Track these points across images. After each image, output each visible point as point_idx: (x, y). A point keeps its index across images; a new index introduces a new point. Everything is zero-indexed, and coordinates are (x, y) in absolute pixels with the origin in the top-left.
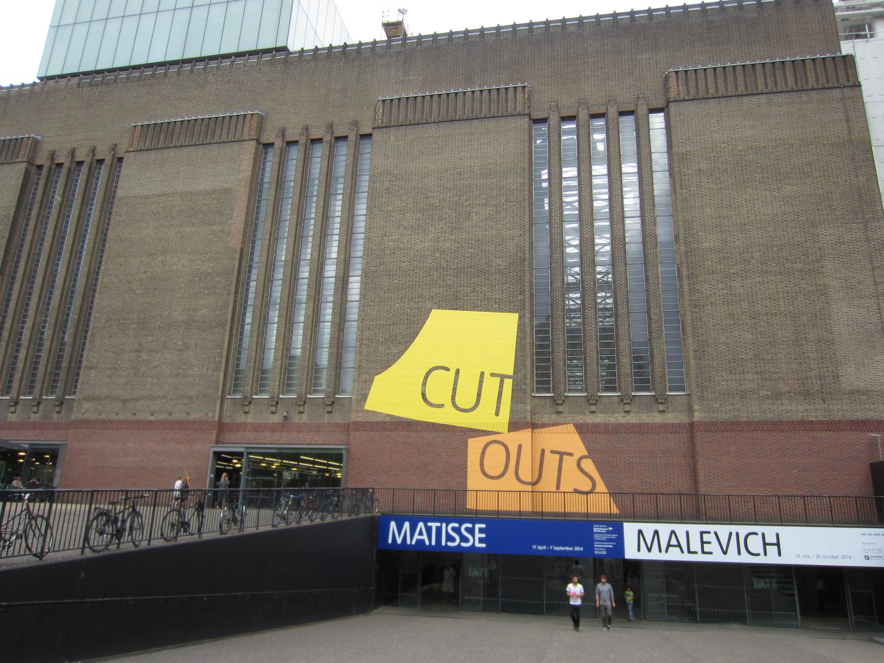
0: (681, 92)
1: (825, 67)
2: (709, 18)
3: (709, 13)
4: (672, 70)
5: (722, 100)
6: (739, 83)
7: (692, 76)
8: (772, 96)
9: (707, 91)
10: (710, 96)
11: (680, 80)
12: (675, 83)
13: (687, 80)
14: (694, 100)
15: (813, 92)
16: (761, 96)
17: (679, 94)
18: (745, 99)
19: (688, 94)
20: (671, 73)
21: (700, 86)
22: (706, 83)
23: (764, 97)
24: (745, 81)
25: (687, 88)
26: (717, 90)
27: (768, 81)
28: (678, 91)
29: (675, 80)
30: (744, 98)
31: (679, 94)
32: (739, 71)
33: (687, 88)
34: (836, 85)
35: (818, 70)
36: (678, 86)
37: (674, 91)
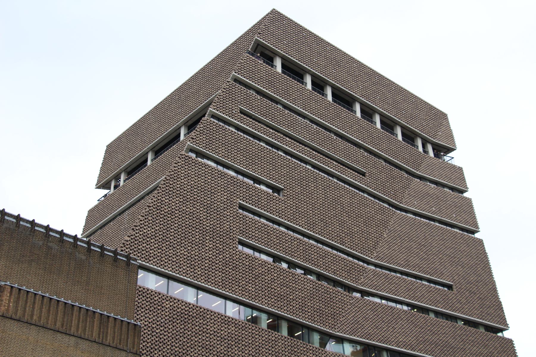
0: (11, 308)
1: (121, 329)
2: (49, 244)
3: (50, 239)
4: (8, 283)
5: (42, 330)
6: (58, 318)
7: (23, 296)
8: (80, 341)
9: (32, 315)
10: (33, 322)
11: (13, 297)
12: (8, 298)
13: (18, 298)
14: (19, 320)
15: (109, 348)
16: (71, 338)
17: (8, 310)
18: (59, 336)
19: (16, 314)
20: (7, 287)
21: (27, 309)
22: (33, 308)
23: (73, 339)
24: (63, 318)
25: (17, 307)
26: (40, 318)
27: (80, 326)
28: (9, 306)
29: (8, 295)
30: (59, 335)
31: (8, 310)
32: (61, 307)
33: (17, 307)
34: (125, 348)
35: (116, 330)
36: (9, 301)
37: (5, 306)
